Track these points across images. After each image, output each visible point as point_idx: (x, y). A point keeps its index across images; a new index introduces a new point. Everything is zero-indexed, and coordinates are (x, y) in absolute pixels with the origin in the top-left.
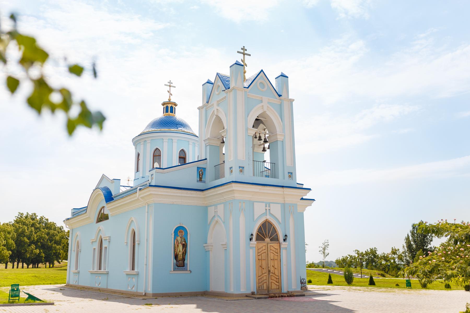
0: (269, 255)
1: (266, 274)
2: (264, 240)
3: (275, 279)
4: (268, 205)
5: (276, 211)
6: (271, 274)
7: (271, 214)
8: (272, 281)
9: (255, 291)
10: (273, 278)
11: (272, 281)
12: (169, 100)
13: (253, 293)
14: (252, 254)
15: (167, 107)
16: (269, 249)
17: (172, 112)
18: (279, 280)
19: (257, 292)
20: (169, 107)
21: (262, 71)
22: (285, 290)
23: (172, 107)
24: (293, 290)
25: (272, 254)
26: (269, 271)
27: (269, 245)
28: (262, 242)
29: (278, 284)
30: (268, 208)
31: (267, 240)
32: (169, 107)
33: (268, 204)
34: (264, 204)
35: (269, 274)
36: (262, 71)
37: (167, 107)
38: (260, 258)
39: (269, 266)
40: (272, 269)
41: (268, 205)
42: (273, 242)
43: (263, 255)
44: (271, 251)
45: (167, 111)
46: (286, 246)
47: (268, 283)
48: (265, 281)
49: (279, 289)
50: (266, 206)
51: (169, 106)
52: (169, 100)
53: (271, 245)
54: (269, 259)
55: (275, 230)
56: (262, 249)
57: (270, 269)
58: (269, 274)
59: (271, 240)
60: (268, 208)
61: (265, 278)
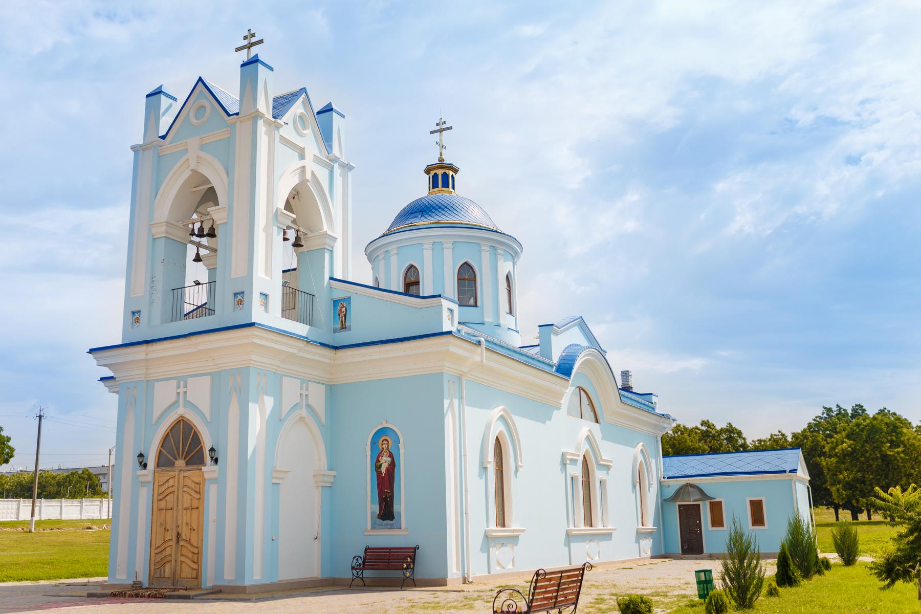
0: (180, 497)
1: (170, 543)
2: (172, 464)
3: (190, 555)
4: (182, 383)
5: (200, 394)
6: (182, 543)
7: (188, 404)
8: (183, 559)
9: (144, 579)
10: (185, 551)
11: (183, 559)
12: (441, 160)
13: (137, 585)
14: (145, 496)
15: (435, 176)
16: (181, 486)
17: (446, 185)
18: (197, 557)
19: (150, 584)
20: (441, 175)
21: (200, 79)
22: (209, 580)
23: (445, 176)
24: (225, 584)
25: (186, 496)
26: (178, 535)
27: (182, 474)
28: (168, 468)
29: (195, 566)
30: (181, 390)
31: (180, 463)
32: (441, 175)
33: (182, 381)
34: (174, 382)
35: (178, 541)
36: (200, 79)
37: (435, 176)
38: (162, 504)
39: (180, 522)
40: (185, 532)
41: (182, 383)
42: (190, 467)
43: (168, 498)
44: (185, 489)
45: (435, 185)
46: (215, 475)
47: (173, 562)
48: (169, 559)
49: (196, 578)
50: (178, 387)
51: (440, 172)
52: (441, 160)
53: (186, 474)
54: (180, 507)
55: (196, 440)
56: (166, 486)
57: (180, 530)
58: (178, 541)
59: (188, 464)
60: (181, 390)
61: (168, 552)
